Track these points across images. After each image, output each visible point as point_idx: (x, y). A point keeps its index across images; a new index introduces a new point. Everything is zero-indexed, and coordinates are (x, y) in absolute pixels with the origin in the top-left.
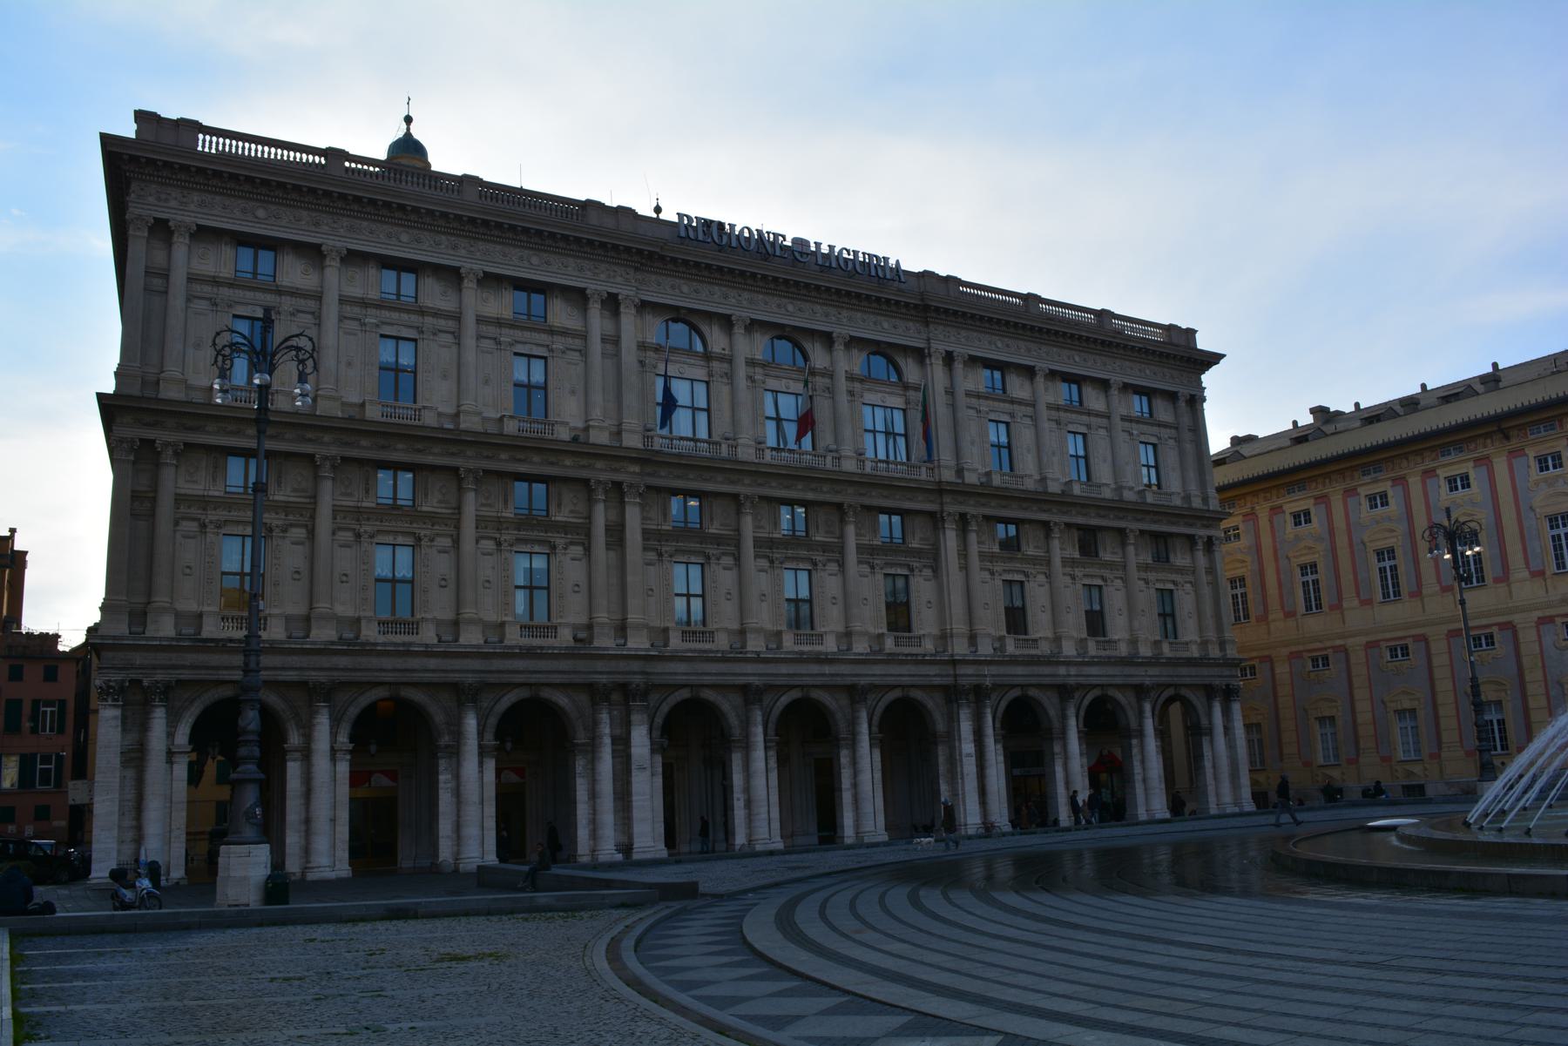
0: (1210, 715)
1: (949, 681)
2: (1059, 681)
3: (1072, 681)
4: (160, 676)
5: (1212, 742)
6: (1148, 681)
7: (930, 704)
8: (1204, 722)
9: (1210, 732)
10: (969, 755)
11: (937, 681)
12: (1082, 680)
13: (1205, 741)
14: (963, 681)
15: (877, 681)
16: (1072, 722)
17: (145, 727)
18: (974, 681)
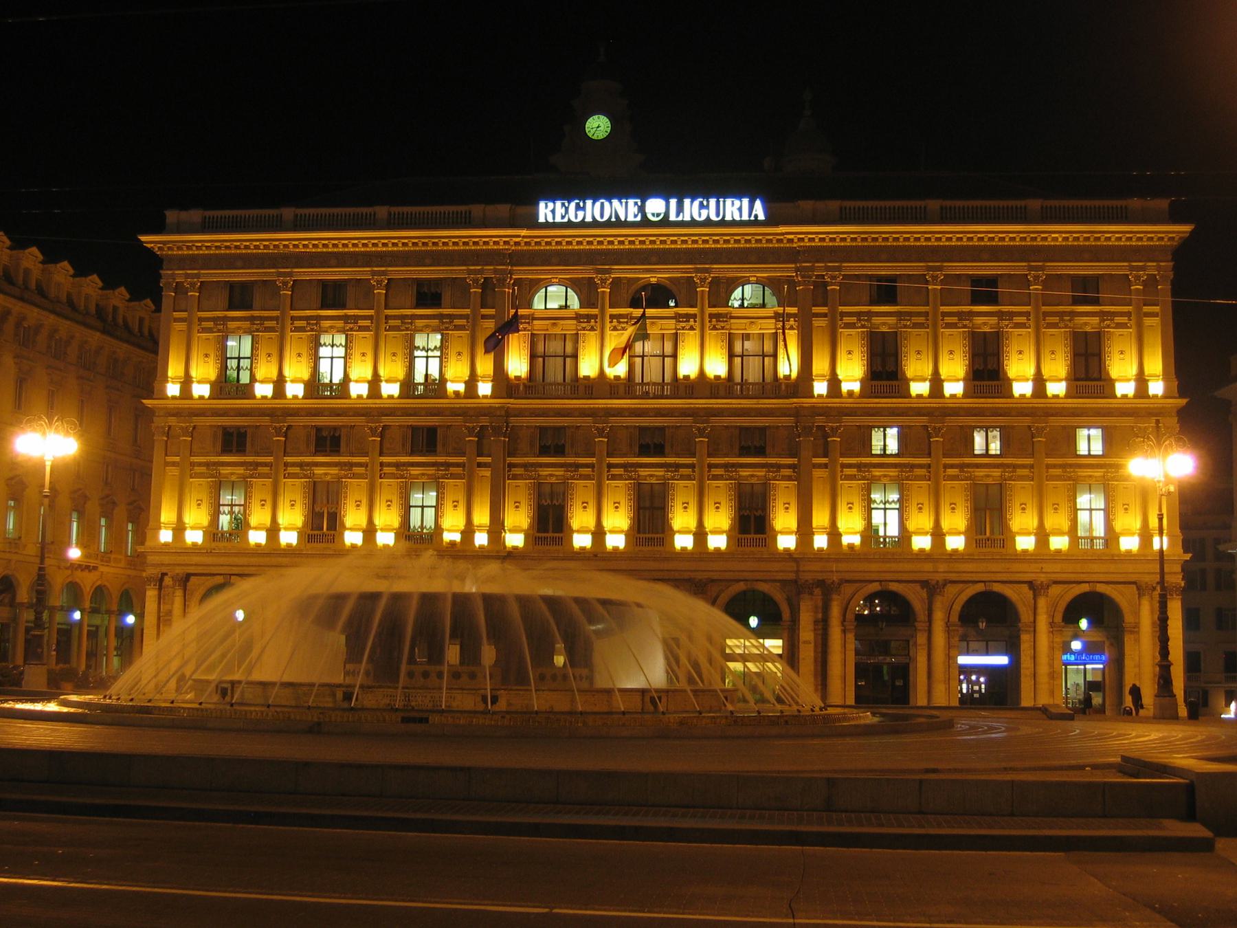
0: (1137, 614)
1: (792, 576)
2: (925, 577)
3: (940, 577)
4: (178, 570)
5: (1137, 641)
6: (1042, 578)
7: (779, 597)
8: (1129, 618)
9: (1136, 629)
10: (805, 642)
11: (780, 576)
12: (953, 577)
13: (1128, 640)
14: (808, 577)
15: (715, 576)
16: (939, 616)
17: (173, 603)
18: (820, 577)
